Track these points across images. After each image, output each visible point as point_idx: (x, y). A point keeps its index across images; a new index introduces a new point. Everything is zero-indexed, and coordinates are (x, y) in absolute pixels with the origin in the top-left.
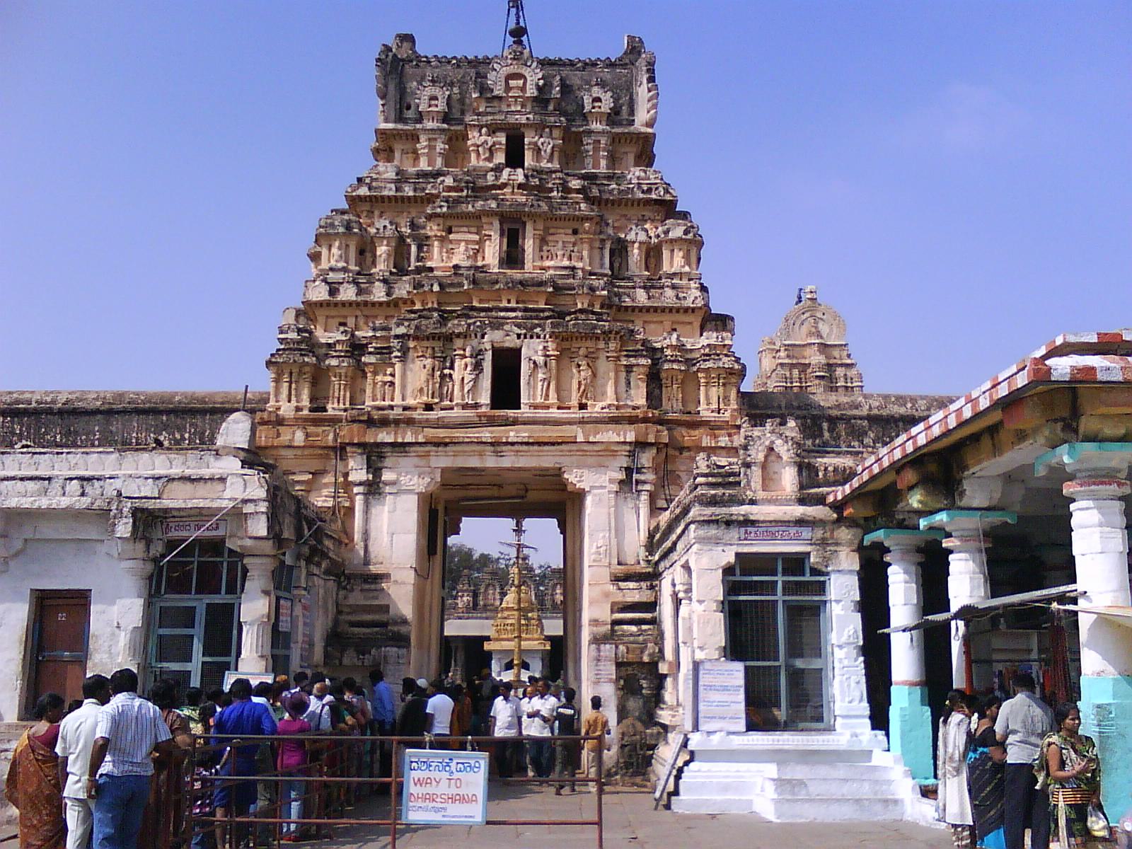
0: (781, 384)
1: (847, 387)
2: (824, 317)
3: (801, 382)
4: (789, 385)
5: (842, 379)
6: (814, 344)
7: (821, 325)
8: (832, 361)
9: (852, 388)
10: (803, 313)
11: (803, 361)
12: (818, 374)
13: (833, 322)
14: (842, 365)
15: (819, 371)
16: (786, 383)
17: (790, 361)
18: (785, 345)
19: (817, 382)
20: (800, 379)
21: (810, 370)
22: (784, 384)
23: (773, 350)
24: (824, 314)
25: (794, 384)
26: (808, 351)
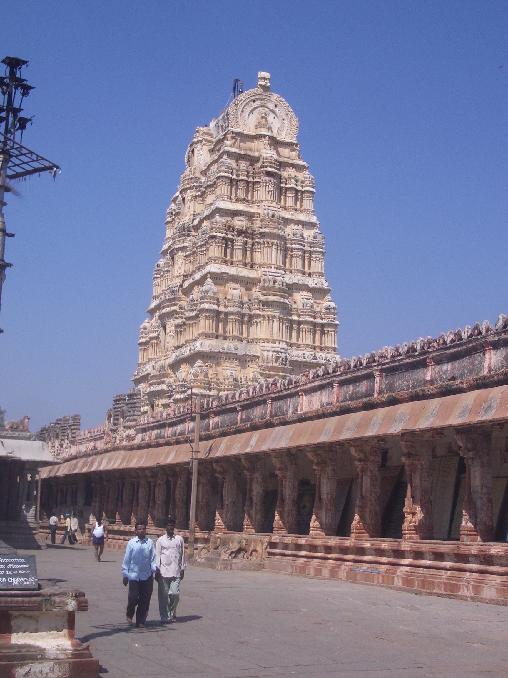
0: (227, 175)
1: (297, 191)
2: (276, 110)
3: (248, 177)
4: (234, 177)
5: (293, 180)
6: (265, 136)
7: (271, 118)
8: (281, 160)
9: (303, 192)
10: (254, 101)
11: (251, 154)
12: (269, 169)
13: (285, 117)
14: (293, 166)
15: (270, 167)
16: (232, 174)
17: (237, 151)
18: (233, 133)
19: (267, 179)
20: (248, 172)
21: (258, 165)
22: (230, 175)
23: (209, 141)
24: (276, 106)
25: (241, 178)
26: (254, 145)
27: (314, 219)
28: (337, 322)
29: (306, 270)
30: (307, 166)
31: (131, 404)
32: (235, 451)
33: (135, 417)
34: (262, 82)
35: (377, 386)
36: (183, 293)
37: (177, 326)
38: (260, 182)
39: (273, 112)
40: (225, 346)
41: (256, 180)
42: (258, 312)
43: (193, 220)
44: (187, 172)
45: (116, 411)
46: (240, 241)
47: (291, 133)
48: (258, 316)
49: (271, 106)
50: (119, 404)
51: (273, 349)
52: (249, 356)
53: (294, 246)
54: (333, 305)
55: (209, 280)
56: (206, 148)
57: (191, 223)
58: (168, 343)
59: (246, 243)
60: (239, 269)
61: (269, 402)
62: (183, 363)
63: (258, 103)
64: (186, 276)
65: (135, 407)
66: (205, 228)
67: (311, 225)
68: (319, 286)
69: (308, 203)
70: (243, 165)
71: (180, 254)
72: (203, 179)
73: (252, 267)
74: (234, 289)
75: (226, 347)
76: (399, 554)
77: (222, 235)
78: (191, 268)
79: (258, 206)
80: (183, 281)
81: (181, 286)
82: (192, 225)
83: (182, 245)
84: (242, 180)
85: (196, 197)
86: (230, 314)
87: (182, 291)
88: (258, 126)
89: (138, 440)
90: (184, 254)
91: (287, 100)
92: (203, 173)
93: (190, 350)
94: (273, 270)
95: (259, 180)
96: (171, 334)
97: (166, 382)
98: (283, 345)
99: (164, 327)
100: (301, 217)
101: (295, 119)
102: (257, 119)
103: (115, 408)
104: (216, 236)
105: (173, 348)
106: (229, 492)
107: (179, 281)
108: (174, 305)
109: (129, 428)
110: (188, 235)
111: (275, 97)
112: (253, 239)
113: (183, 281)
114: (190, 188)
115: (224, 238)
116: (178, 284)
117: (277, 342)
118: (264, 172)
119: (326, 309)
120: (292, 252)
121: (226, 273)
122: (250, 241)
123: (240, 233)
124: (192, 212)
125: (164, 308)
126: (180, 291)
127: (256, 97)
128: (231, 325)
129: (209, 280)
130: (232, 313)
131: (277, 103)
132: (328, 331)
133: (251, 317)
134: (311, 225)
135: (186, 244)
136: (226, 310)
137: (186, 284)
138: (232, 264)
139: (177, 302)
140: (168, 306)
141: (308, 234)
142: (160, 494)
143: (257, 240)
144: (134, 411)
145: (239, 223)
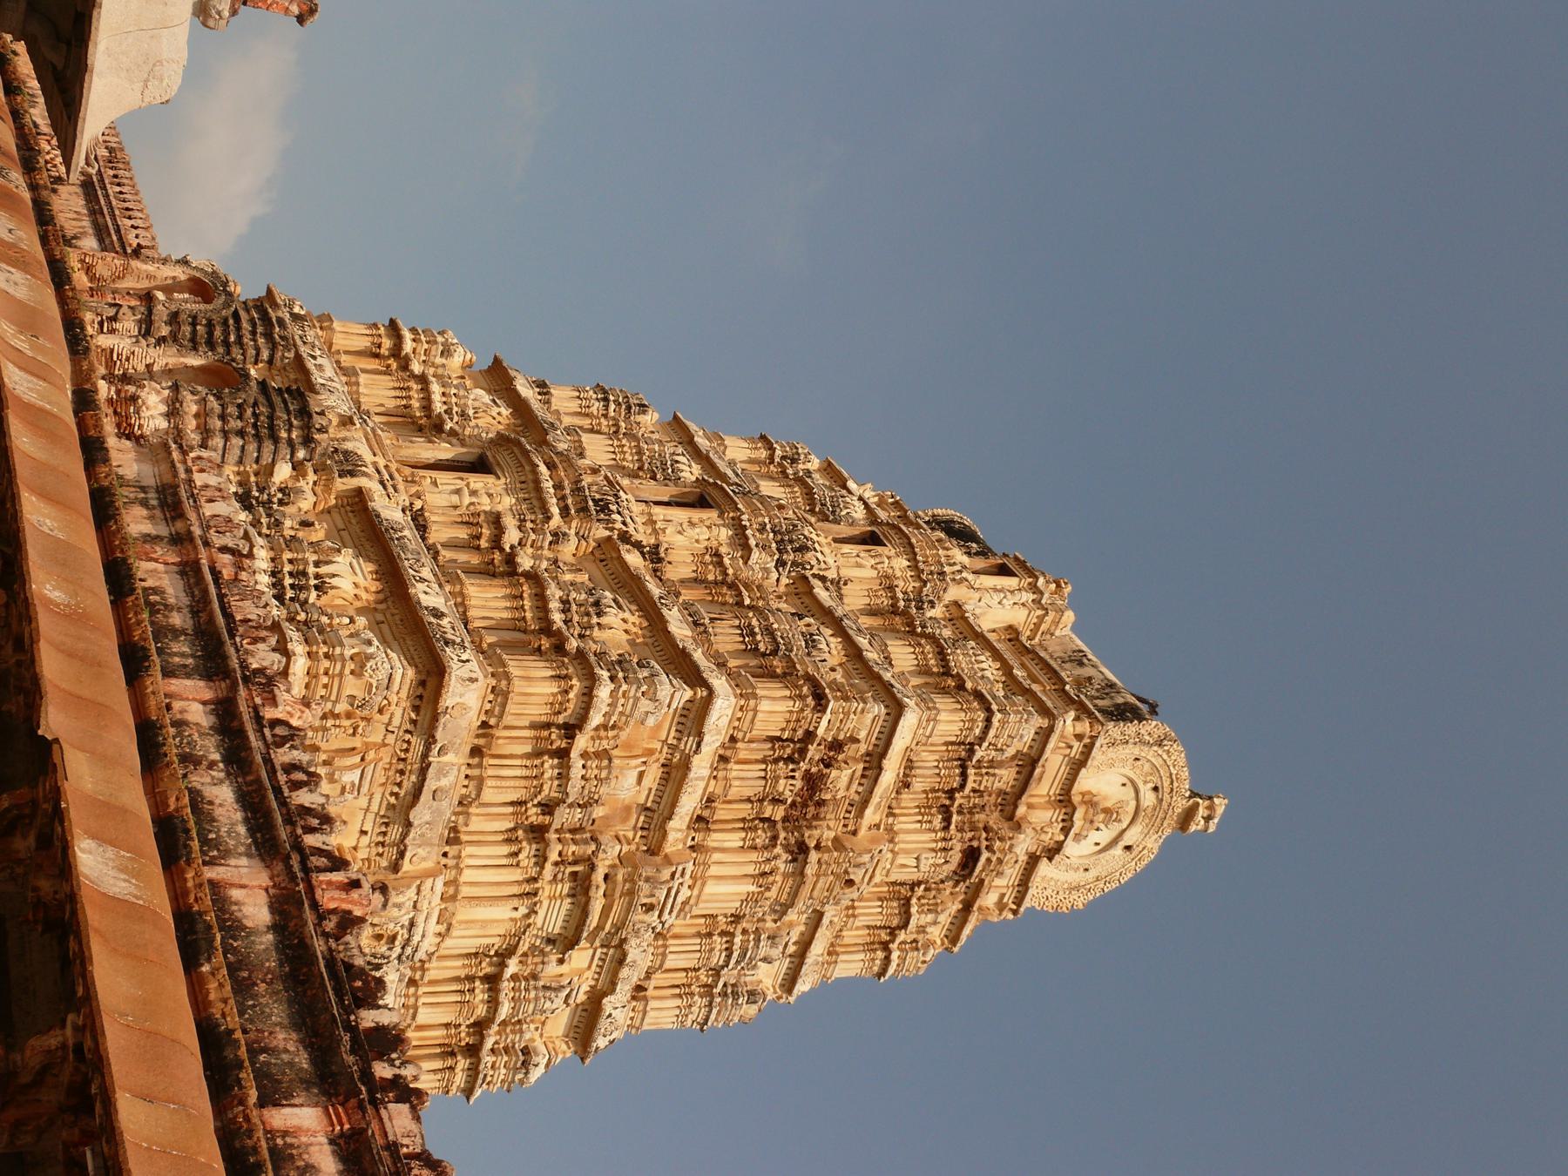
2: (1118, 851)
9: (885, 946)
12: (985, 855)
24: (1128, 848)
27: (803, 986)
28: (478, 1093)
29: (658, 979)
30: (956, 950)
31: (271, 418)
33: (218, 441)
34: (1202, 812)
36: (600, 544)
37: (496, 520)
38: (946, 828)
39: (1114, 842)
40: (449, 758)
41: (955, 818)
42: (553, 856)
43: (823, 579)
44: (959, 556)
45: (225, 322)
46: (789, 788)
47: (1048, 892)
48: (541, 859)
49: (1130, 838)
50: (254, 333)
51: (420, 920)
52: (404, 836)
53: (738, 940)
54: (536, 1074)
55: (689, 694)
56: (1019, 617)
57: (815, 571)
58: (435, 483)
59: (776, 801)
60: (702, 784)
62: (380, 575)
63: (1149, 799)
64: (654, 556)
65: (258, 437)
66: (823, 646)
67: (790, 982)
68: (603, 1024)
69: (851, 966)
70: (1006, 777)
71: (725, 534)
73: (700, 819)
74: (641, 775)
75: (445, 759)
77: (820, 732)
79: (877, 826)
80: (638, 545)
81: (625, 537)
82: (808, 573)
83: (752, 542)
84: (964, 775)
85: (891, 588)
86: (560, 766)
87: (609, 538)
88: (1090, 801)
89: (125, 460)
90: (723, 550)
91: (1138, 878)
92: (953, 609)
93: (438, 614)
94: (685, 893)
95: (953, 827)
96: (467, 500)
97: (302, 483)
98: (428, 945)
99: (479, 466)
100: (818, 948)
101: (1080, 900)
102: (1105, 798)
103: (236, 315)
104: (824, 711)
105: (418, 505)
107: (642, 535)
108: (565, 512)
109: (173, 412)
110: (781, 563)
111: (1153, 844)
112: (785, 819)
113: (638, 545)
114: (914, 566)
115: (810, 736)
116: (631, 530)
117: (442, 928)
118: (975, 844)
119: (526, 1051)
120: (723, 933)
121: (699, 745)
122: (779, 813)
123: (814, 783)
124: (845, 573)
125: (551, 466)
126: (607, 533)
127: (1167, 797)
128: (518, 772)
129: (689, 694)
130: (563, 777)
131: (1136, 851)
132: (451, 1068)
133: (538, 833)
134: (790, 982)
135: (755, 555)
136: (574, 754)
137: (633, 559)
138: (723, 759)
139: (574, 524)
140: (558, 487)
141: (767, 976)
143: (782, 835)
144: (241, 433)
145: (842, 780)
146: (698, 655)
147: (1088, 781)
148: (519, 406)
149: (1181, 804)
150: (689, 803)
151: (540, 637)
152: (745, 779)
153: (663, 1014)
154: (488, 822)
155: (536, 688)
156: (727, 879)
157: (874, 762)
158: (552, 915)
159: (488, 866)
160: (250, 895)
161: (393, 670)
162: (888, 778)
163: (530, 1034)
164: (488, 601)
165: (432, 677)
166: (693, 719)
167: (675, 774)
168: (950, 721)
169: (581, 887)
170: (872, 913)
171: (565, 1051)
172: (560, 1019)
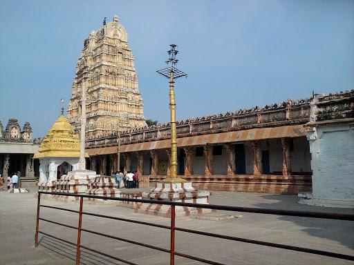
32: (134, 150)
35: (191, 130)
61: (144, 134)
64: (89, 88)
69: (133, 64)
72: (94, 53)
76: (205, 179)
78: (90, 85)
88: (114, 35)
106: (128, 163)
137: (89, 91)
141: (133, 74)
142: (104, 164)
146: (98, 87)
147: (111, 36)
148: (75, 98)
149: (115, 22)
150: (113, 87)
151: (96, 104)
152: (110, 81)
153: (136, 86)
154: (114, 108)
155: (100, 105)
156: (121, 82)
157: (108, 66)
158: (124, 101)
159: (119, 108)
160: (107, 141)
161: (99, 119)
162: (110, 64)
163: (138, 100)
164: (94, 108)
165: (99, 116)
166: (103, 88)
167: (109, 89)
168: (104, 57)
169: (121, 98)
170: (127, 62)
171: (140, 96)
172: (137, 97)
